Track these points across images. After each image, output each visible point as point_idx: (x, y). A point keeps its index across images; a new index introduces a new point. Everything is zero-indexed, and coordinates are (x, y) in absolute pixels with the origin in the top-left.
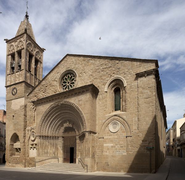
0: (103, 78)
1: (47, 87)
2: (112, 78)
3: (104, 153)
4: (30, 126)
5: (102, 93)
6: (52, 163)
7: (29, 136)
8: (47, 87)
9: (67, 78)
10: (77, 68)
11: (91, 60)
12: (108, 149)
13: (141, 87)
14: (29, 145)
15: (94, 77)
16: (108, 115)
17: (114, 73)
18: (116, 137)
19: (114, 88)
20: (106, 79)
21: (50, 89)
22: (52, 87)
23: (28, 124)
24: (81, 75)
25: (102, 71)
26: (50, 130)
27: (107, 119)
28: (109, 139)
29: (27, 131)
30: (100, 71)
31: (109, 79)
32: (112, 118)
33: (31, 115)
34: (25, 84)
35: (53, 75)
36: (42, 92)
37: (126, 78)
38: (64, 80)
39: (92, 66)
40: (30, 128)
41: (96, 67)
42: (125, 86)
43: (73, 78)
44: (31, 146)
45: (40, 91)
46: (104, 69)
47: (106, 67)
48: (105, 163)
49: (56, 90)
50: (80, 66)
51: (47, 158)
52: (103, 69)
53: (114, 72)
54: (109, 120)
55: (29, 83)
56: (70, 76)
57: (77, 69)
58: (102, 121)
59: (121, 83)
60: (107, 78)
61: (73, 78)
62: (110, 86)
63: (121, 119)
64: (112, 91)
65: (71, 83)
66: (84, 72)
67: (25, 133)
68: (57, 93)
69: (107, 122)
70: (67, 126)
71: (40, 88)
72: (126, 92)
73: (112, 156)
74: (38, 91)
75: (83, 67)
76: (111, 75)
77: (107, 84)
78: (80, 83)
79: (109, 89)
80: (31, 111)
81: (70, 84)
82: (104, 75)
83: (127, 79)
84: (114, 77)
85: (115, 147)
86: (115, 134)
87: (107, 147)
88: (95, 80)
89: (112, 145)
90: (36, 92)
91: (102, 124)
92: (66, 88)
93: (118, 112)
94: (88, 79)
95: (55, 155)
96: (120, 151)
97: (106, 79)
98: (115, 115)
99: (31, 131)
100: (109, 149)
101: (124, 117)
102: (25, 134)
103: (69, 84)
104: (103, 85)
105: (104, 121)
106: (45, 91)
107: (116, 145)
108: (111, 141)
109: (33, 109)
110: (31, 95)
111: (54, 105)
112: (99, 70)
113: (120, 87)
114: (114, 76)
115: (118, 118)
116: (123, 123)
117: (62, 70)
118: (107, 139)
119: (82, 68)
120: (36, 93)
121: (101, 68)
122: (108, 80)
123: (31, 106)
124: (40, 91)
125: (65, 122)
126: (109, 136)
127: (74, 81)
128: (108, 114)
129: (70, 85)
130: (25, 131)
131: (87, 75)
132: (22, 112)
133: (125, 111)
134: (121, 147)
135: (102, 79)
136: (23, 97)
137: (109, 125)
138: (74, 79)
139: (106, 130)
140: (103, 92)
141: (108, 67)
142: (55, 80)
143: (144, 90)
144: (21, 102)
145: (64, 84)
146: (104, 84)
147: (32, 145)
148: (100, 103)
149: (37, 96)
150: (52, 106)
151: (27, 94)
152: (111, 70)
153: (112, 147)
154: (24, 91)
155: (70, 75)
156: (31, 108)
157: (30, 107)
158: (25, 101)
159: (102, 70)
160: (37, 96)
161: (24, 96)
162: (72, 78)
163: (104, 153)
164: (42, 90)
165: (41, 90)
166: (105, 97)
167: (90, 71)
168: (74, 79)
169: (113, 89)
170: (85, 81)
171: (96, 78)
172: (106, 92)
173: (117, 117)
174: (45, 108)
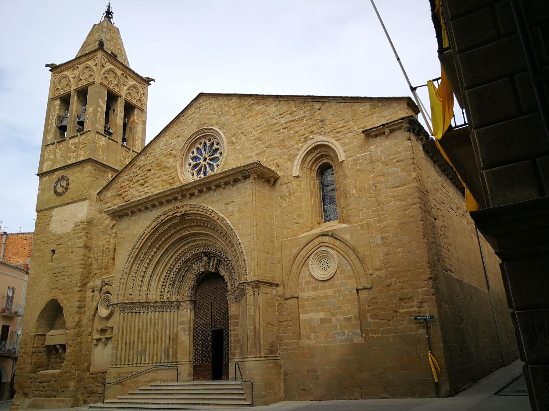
0: (288, 143)
2: (310, 144)
3: (304, 342)
4: (101, 276)
5: (287, 181)
6: (158, 383)
7: (94, 304)
8: (150, 170)
9: (201, 147)
10: (224, 124)
11: (258, 103)
12: (313, 329)
13: (378, 161)
14: (95, 331)
15: (265, 142)
16: (306, 235)
17: (312, 132)
18: (330, 291)
19: (317, 167)
20: (295, 147)
21: (158, 175)
22: (164, 171)
23: (93, 272)
24: (235, 141)
25: (283, 129)
26: (154, 284)
27: (302, 244)
28: (313, 299)
29: (91, 290)
30: (281, 127)
31: (302, 147)
32: (316, 241)
33: (106, 246)
35: (167, 141)
36: (137, 184)
37: (342, 141)
38: (193, 153)
39: (260, 118)
40: (98, 282)
41: (269, 120)
42: (340, 160)
43: (215, 146)
44: (97, 336)
45: (131, 181)
46: (288, 125)
47: (293, 118)
48: (309, 371)
49: (173, 178)
50: (232, 119)
51: (143, 369)
52: (286, 123)
53: (313, 129)
54: (309, 247)
56: (208, 144)
57: (225, 127)
58: (291, 251)
59: (332, 154)
60: (297, 143)
61: (215, 146)
62: (307, 162)
63: (337, 243)
64: (314, 174)
65: (211, 160)
66: (242, 133)
67: (85, 298)
68: (175, 186)
69: (303, 253)
70: (203, 270)
71: (131, 175)
72: (346, 176)
73: (325, 348)
74: (127, 183)
75: (239, 121)
76: (307, 137)
77: (298, 158)
78: (232, 157)
79: (304, 171)
80: (104, 234)
81: (208, 161)
82: (290, 137)
83: (343, 145)
84: (314, 141)
85: (329, 321)
86: (327, 284)
87: (309, 321)
88: (268, 150)
89: (322, 315)
90: (123, 184)
91: (292, 258)
92: (199, 172)
93: (333, 226)
94: (251, 148)
95: (168, 356)
96: (344, 334)
97: (295, 147)
98: (323, 235)
99: (101, 289)
100: (314, 327)
101: (347, 237)
102: (82, 300)
103: (206, 163)
104: (289, 160)
105: (295, 251)
106: (145, 182)
107: (334, 314)
108: (318, 305)
109: (112, 228)
110: (109, 194)
111: (163, 217)
112: (277, 125)
113: (331, 163)
114: (312, 139)
115: (332, 240)
116: (344, 254)
117: (188, 129)
118: (308, 300)
119: (236, 124)
120: (122, 187)
121: (282, 121)
122: (299, 150)
123: (107, 221)
124: (131, 181)
125: (197, 258)
126: (312, 291)
127: (217, 155)
128: (307, 232)
129: (209, 164)
130: (85, 291)
131: (250, 140)
132: (79, 238)
133: (349, 222)
134: (347, 319)
135: (285, 146)
137: (310, 260)
138: (217, 149)
139: (302, 274)
140: (289, 178)
141: (297, 117)
143: (388, 167)
144: (81, 211)
145: (195, 163)
146: (291, 159)
147: (103, 331)
148: (284, 204)
149: (124, 194)
150: (159, 220)
152: (305, 124)
153: (322, 321)
155: (210, 140)
156: (108, 225)
157: (105, 224)
158: (88, 209)
159: (284, 126)
160: (123, 196)
162: (213, 148)
163: (304, 342)
164: (138, 178)
165: (135, 180)
166: (294, 189)
167: (257, 128)
168: (217, 149)
169: (316, 169)
170: (245, 152)
171: (270, 145)
172: (298, 177)
173: (328, 238)
174: (141, 226)
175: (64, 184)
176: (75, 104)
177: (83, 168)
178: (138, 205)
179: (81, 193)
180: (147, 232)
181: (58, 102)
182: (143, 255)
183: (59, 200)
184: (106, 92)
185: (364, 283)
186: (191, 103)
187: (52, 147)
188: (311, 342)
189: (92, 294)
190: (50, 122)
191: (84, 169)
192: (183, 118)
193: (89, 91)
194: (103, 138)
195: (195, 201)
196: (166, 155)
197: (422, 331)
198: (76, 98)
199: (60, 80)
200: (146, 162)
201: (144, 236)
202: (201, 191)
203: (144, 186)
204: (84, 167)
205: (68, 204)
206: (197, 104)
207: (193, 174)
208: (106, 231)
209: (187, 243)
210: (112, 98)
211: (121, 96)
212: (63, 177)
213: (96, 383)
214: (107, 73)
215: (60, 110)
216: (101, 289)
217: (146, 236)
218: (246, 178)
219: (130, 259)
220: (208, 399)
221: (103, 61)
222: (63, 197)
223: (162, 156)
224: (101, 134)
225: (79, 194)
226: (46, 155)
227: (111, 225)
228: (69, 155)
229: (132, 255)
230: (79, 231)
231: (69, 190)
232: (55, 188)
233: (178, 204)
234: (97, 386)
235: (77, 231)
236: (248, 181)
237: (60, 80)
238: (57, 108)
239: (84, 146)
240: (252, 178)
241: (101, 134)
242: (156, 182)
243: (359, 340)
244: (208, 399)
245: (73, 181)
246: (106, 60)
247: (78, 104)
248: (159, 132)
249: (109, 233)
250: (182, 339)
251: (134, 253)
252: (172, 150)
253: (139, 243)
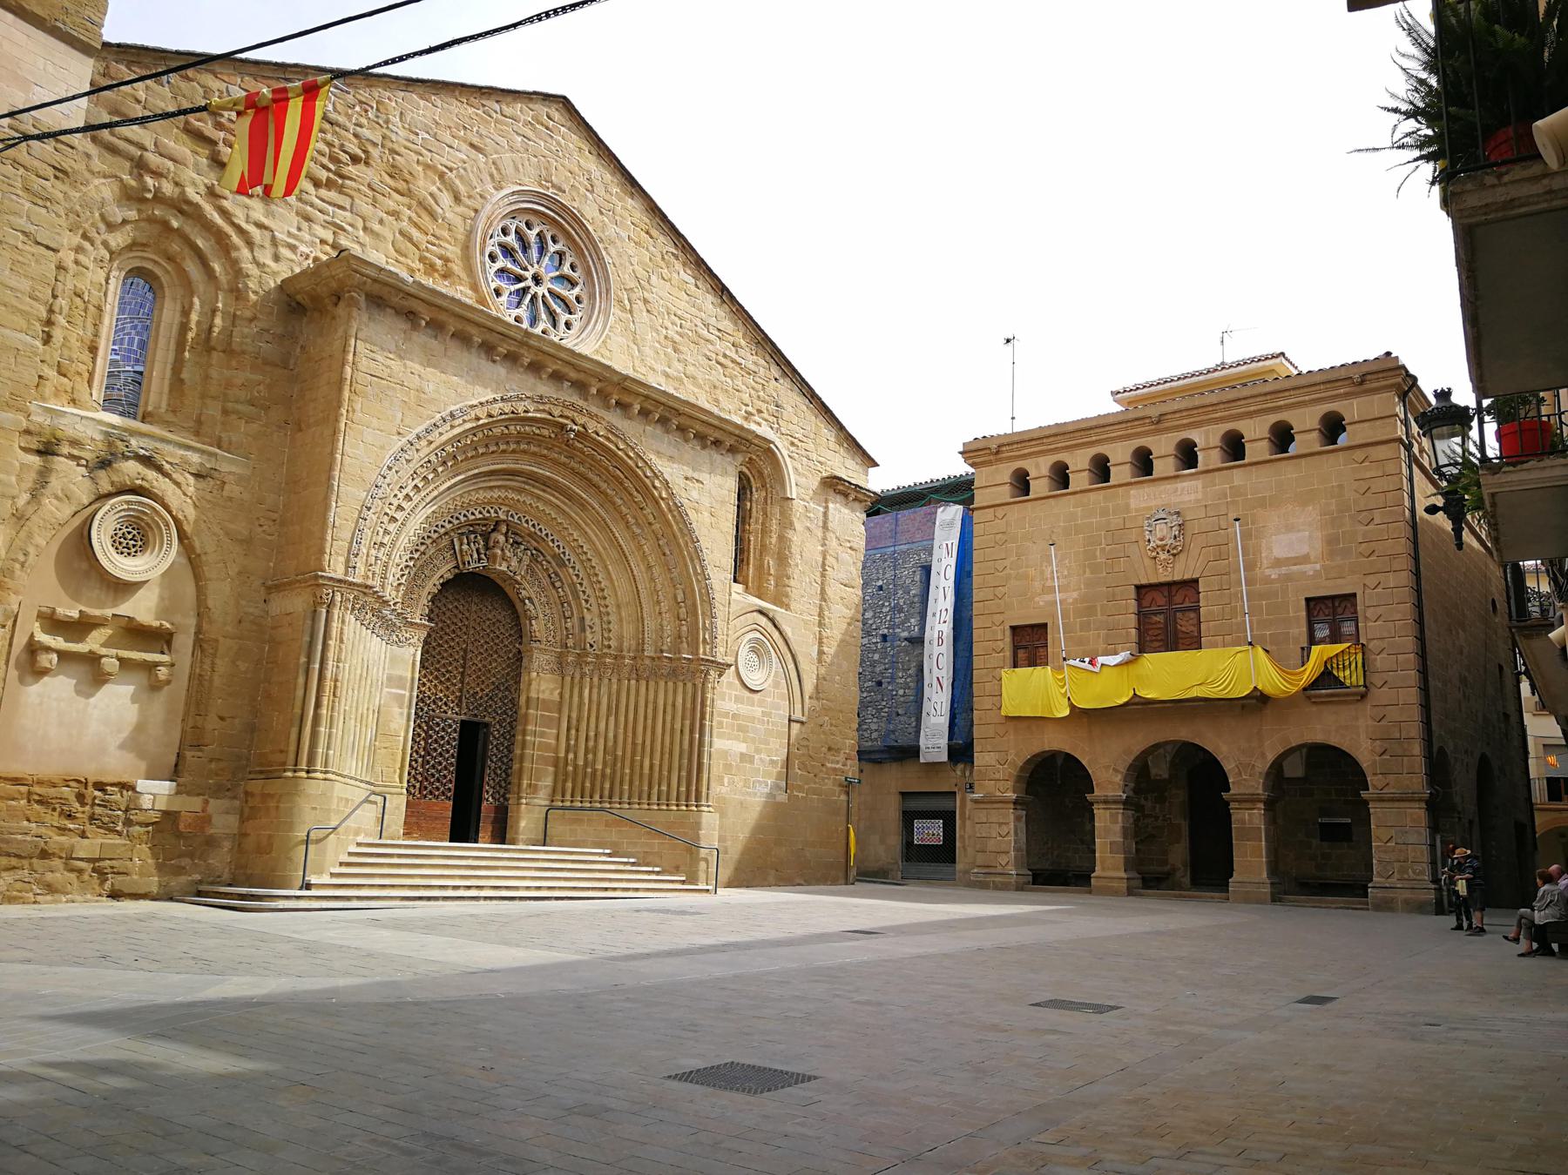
1: (355, 159)
11: (684, 265)
12: (728, 767)
21: (391, 205)
28: (735, 716)
52: (725, 356)
53: (763, 406)
63: (776, 635)
66: (646, 301)
85: (751, 760)
87: (725, 754)
89: (742, 747)
106: (329, 184)
107: (758, 751)
108: (741, 728)
118: (726, 715)
135: (717, 400)
142: (442, 176)
178: (478, 325)
185: (798, 715)
186: (535, 93)
188: (724, 790)
189: (35, 460)
192: (497, 107)
195: (615, 418)
196: (427, 167)
197: (843, 797)
202: (645, 413)
203: (323, 192)
206: (542, 109)
207: (498, 293)
209: (506, 488)
213: (55, 819)
216: (104, 464)
218: (732, 450)
220: (610, 880)
223: (415, 157)
233: (575, 399)
234: (63, 830)
236: (729, 458)
240: (740, 458)
242: (381, 222)
243: (782, 797)
244: (610, 880)
248: (425, 77)
249: (93, 234)
250: (393, 726)
252: (451, 170)
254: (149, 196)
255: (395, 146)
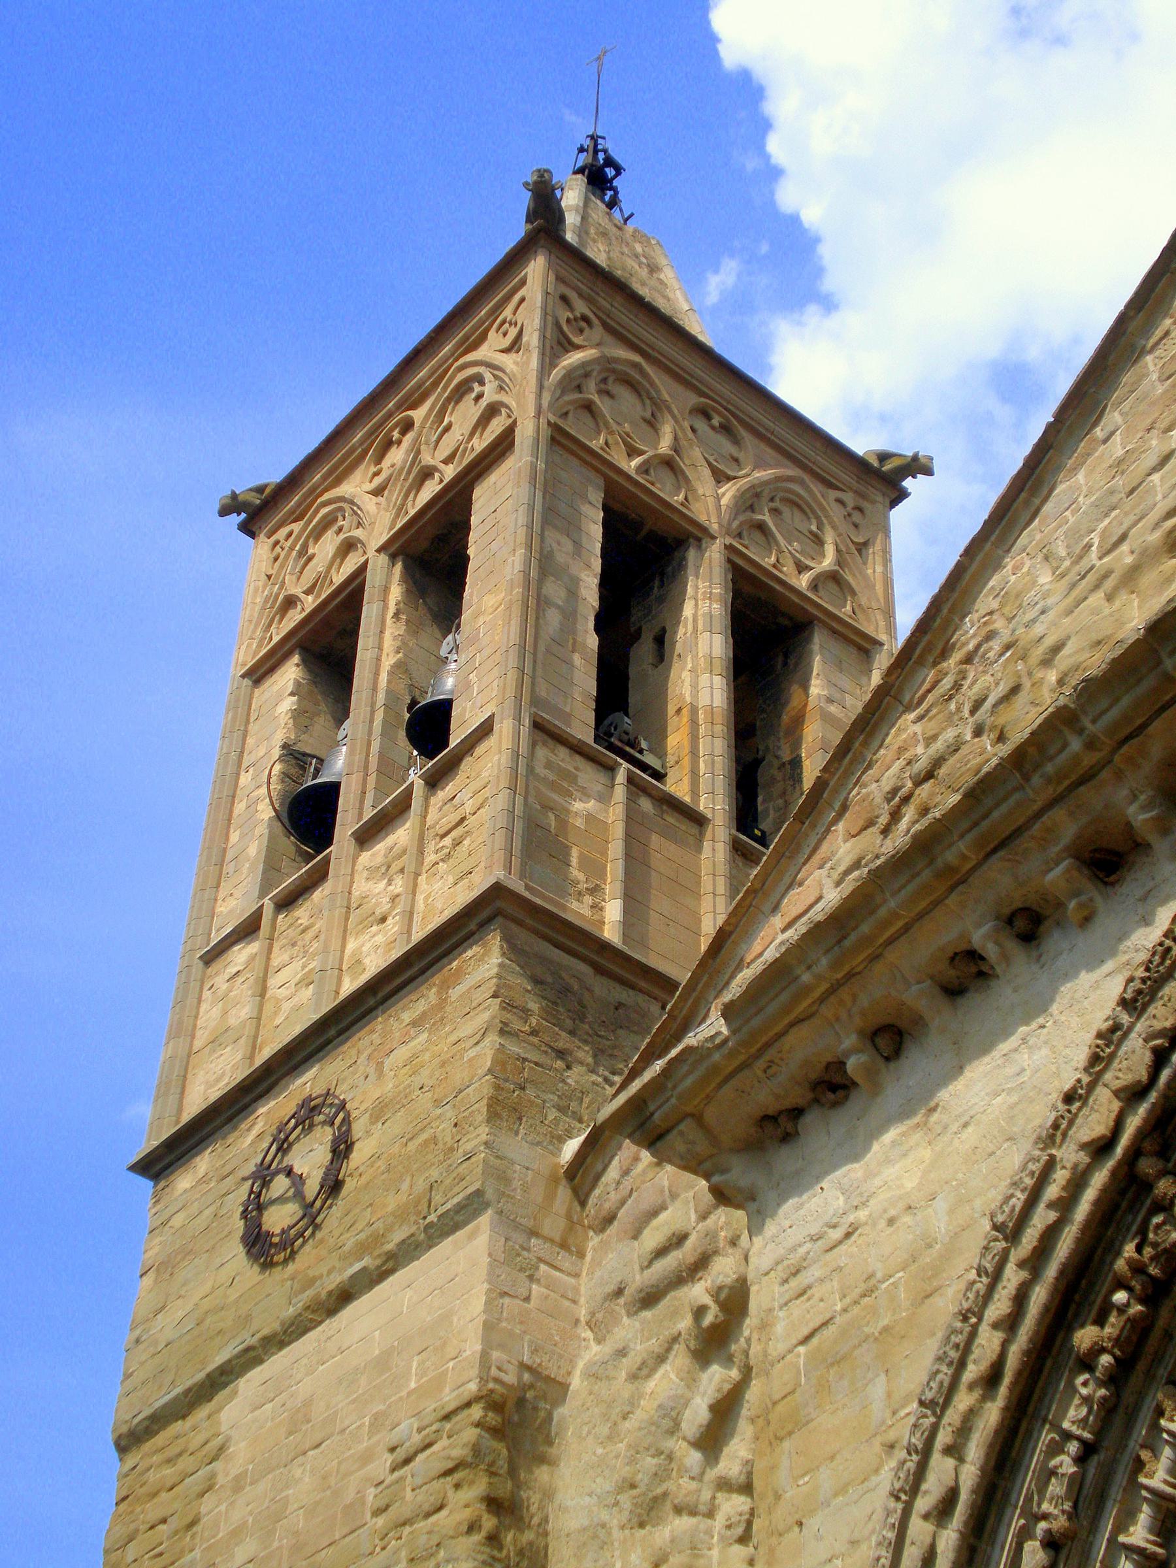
34: (513, 949)
55: (611, 933)
80: (648, 1511)
136: (471, 1207)
151: (572, 1146)
154: (480, 1090)
157: (646, 1409)
161: (499, 1173)
175: (310, 1157)
176: (393, 631)
177: (445, 986)
179: (434, 1174)
180: (1070, 1155)
181: (291, 673)
182: (1065, 1464)
183: (276, 1295)
184: (596, 496)
187: (241, 955)
190: (240, 807)
191: (455, 993)
193: (475, 507)
194: (588, 775)
198: (396, 592)
199: (305, 547)
200: (949, 734)
201: (1042, 1217)
204: (459, 974)
205: (344, 1297)
208: (659, 1476)
210: (641, 558)
211: (697, 535)
212: (308, 1114)
214: (591, 385)
215: (298, 715)
217: (1065, 1205)
219: (919, 1529)
221: (564, 315)
222: (307, 1256)
224: (578, 749)
225: (421, 1184)
226: (209, 1015)
227: (698, 1413)
228: (351, 945)
229: (941, 1469)
230: (426, 1499)
231: (349, 1186)
232: (255, 1208)
235: (411, 1500)
237: (305, 547)
238: (289, 703)
239: (457, 843)
241: (578, 749)
245: (379, 1112)
246: (581, 307)
247: (414, 628)
251: (954, 1450)
253: (1000, 1306)
254: (708, 1320)
255: (1049, 641)
